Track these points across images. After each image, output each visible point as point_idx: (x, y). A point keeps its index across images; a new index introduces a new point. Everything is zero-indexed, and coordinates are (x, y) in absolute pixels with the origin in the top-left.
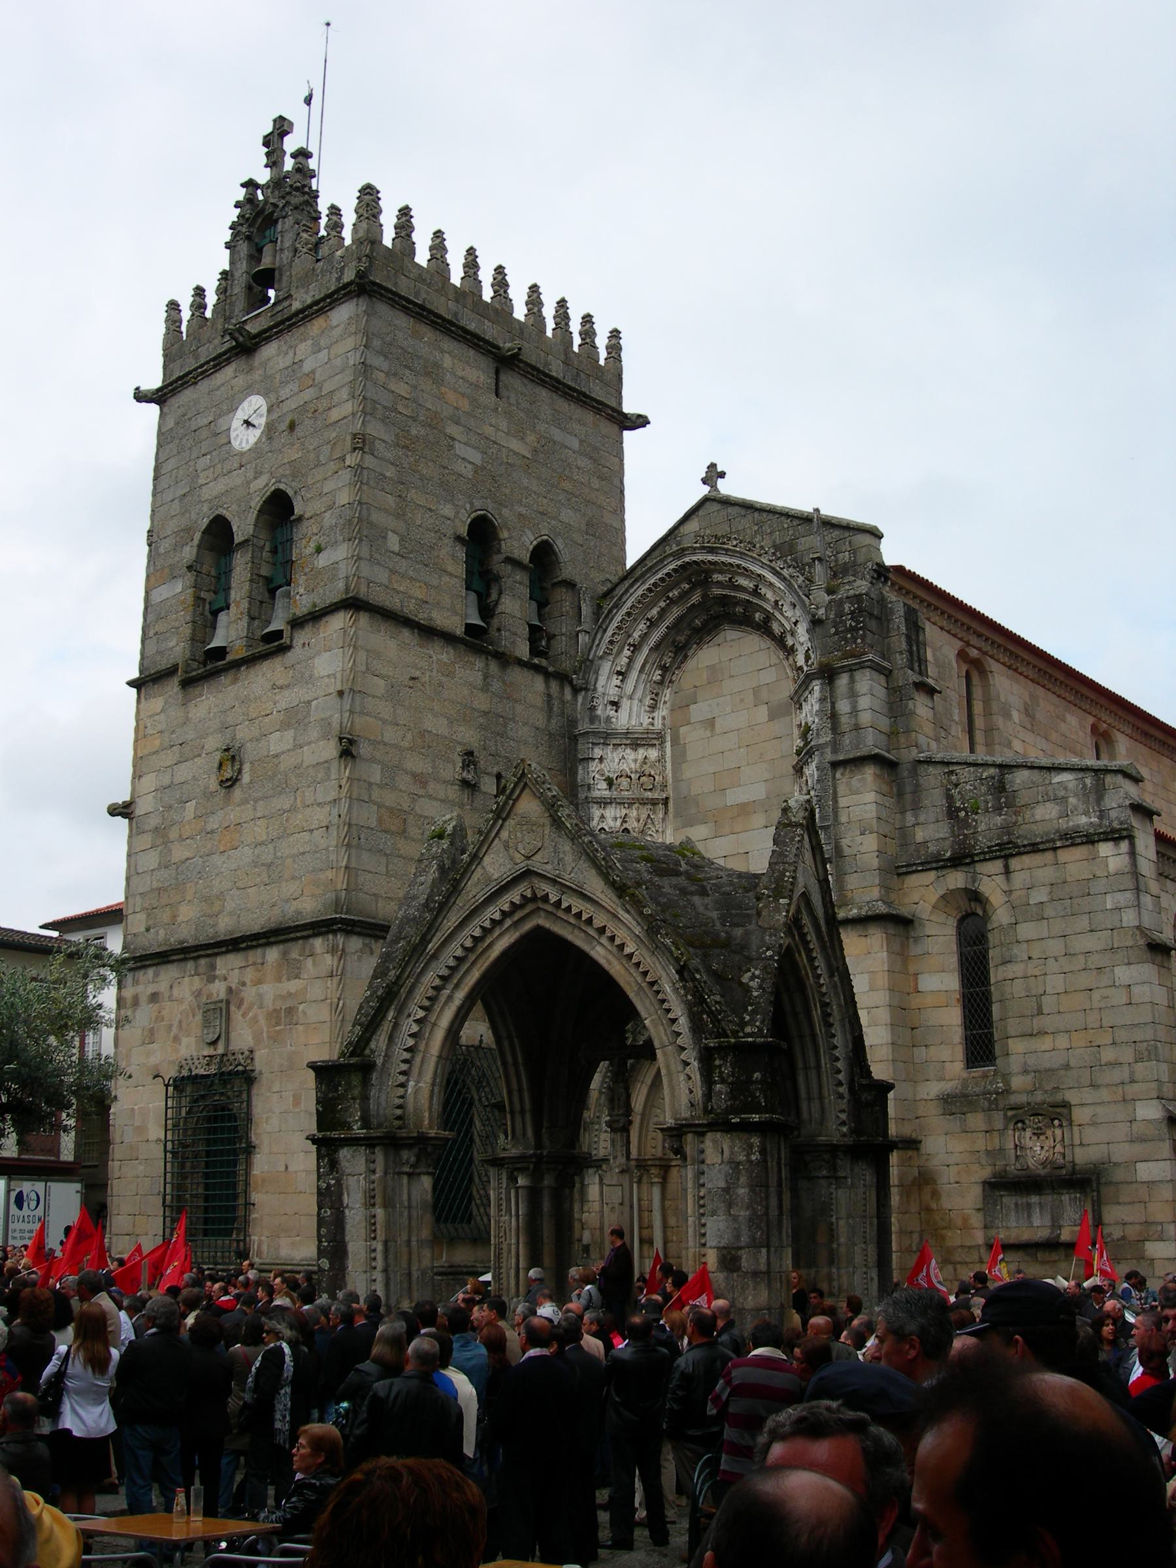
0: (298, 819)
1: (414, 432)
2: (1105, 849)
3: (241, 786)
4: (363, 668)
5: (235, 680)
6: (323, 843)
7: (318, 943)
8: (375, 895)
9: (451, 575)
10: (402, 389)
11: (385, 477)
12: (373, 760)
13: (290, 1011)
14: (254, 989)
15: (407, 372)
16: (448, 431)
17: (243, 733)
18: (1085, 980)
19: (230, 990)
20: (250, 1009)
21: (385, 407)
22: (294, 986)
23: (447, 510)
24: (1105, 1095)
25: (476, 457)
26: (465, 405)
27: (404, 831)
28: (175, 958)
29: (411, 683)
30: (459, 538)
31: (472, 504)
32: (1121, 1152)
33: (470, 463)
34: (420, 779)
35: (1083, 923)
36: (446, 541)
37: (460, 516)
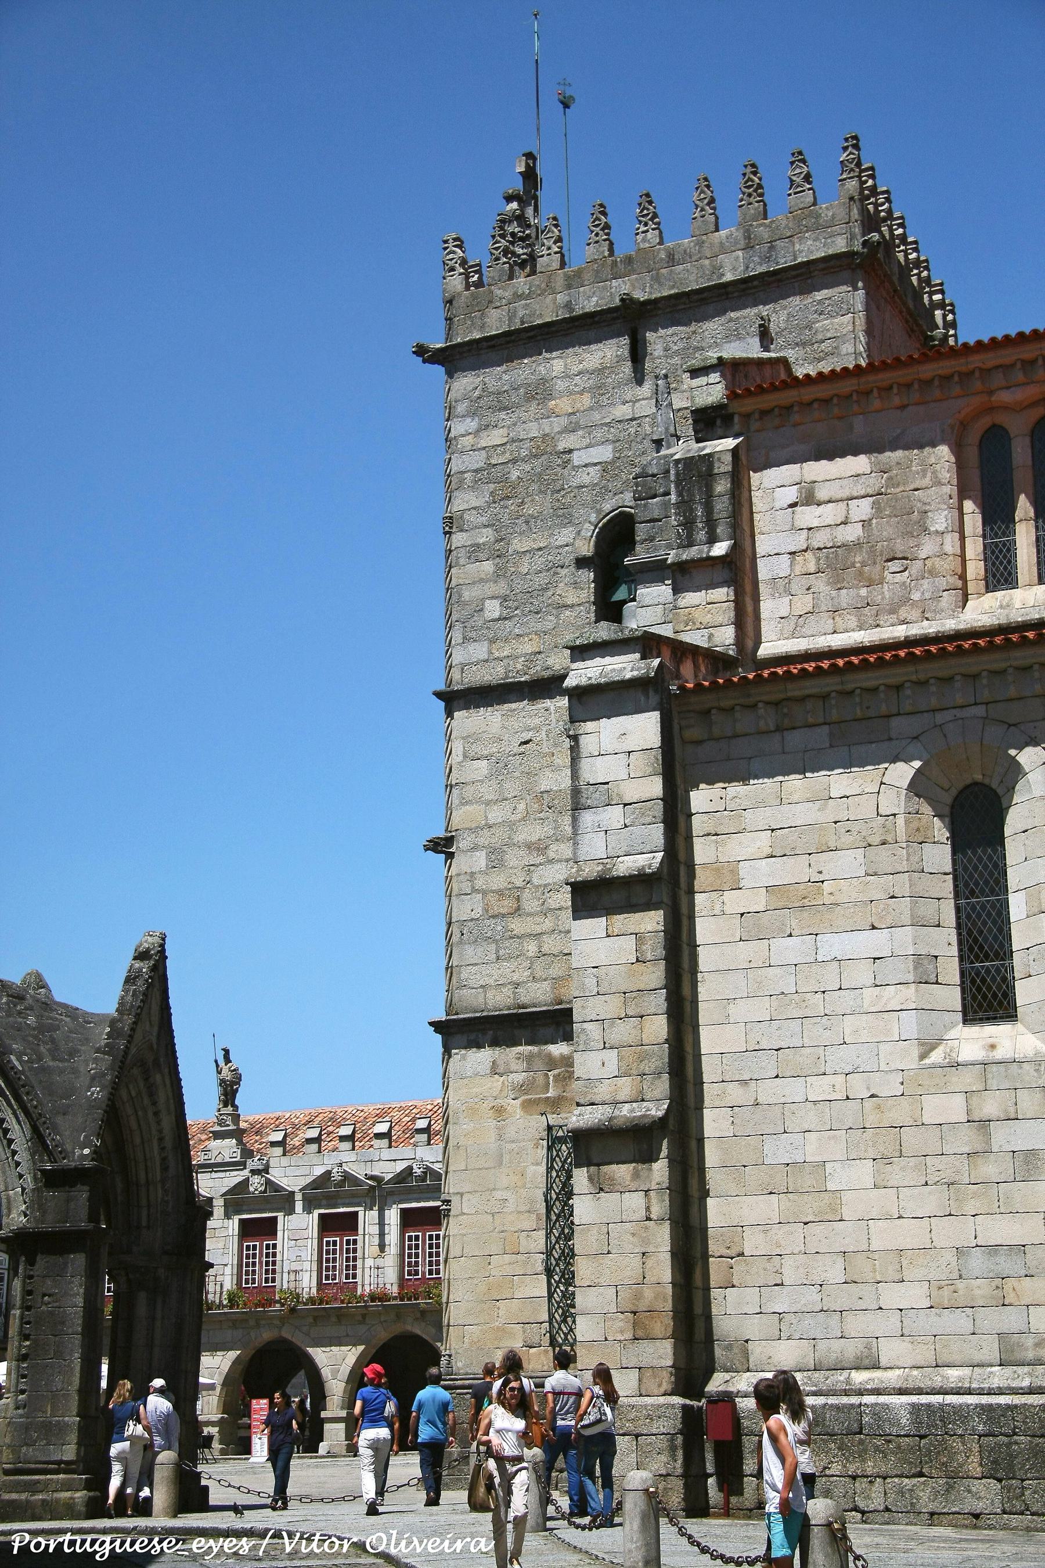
1: (514, 475)
4: (461, 758)
8: (482, 986)
9: (573, 606)
10: (496, 437)
11: (478, 545)
12: (475, 848)
15: (503, 415)
16: (561, 446)
21: (476, 471)
23: (566, 535)
25: (605, 453)
26: (586, 400)
27: (518, 909)
29: (522, 749)
30: (581, 562)
31: (599, 511)
33: (595, 464)
34: (538, 847)
36: (563, 572)
37: (583, 533)
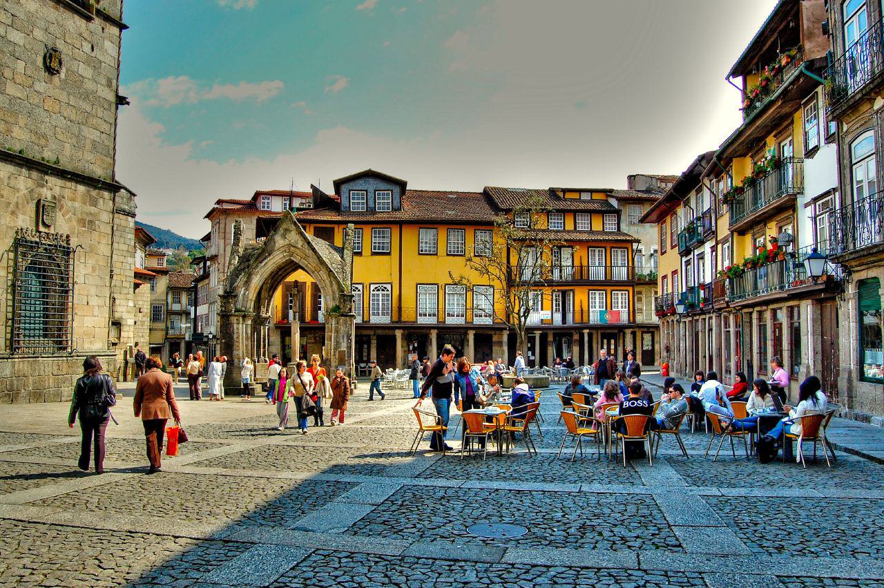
0: (94, 121)
2: (130, 218)
3: (60, 77)
5: (56, 9)
6: (107, 143)
7: (106, 194)
13: (91, 222)
14: (70, 203)
17: (60, 45)
18: (122, 259)
19: (54, 198)
20: (67, 212)
22: (93, 209)
24: (122, 296)
28: (17, 161)
32: (125, 316)
35: (122, 240)
